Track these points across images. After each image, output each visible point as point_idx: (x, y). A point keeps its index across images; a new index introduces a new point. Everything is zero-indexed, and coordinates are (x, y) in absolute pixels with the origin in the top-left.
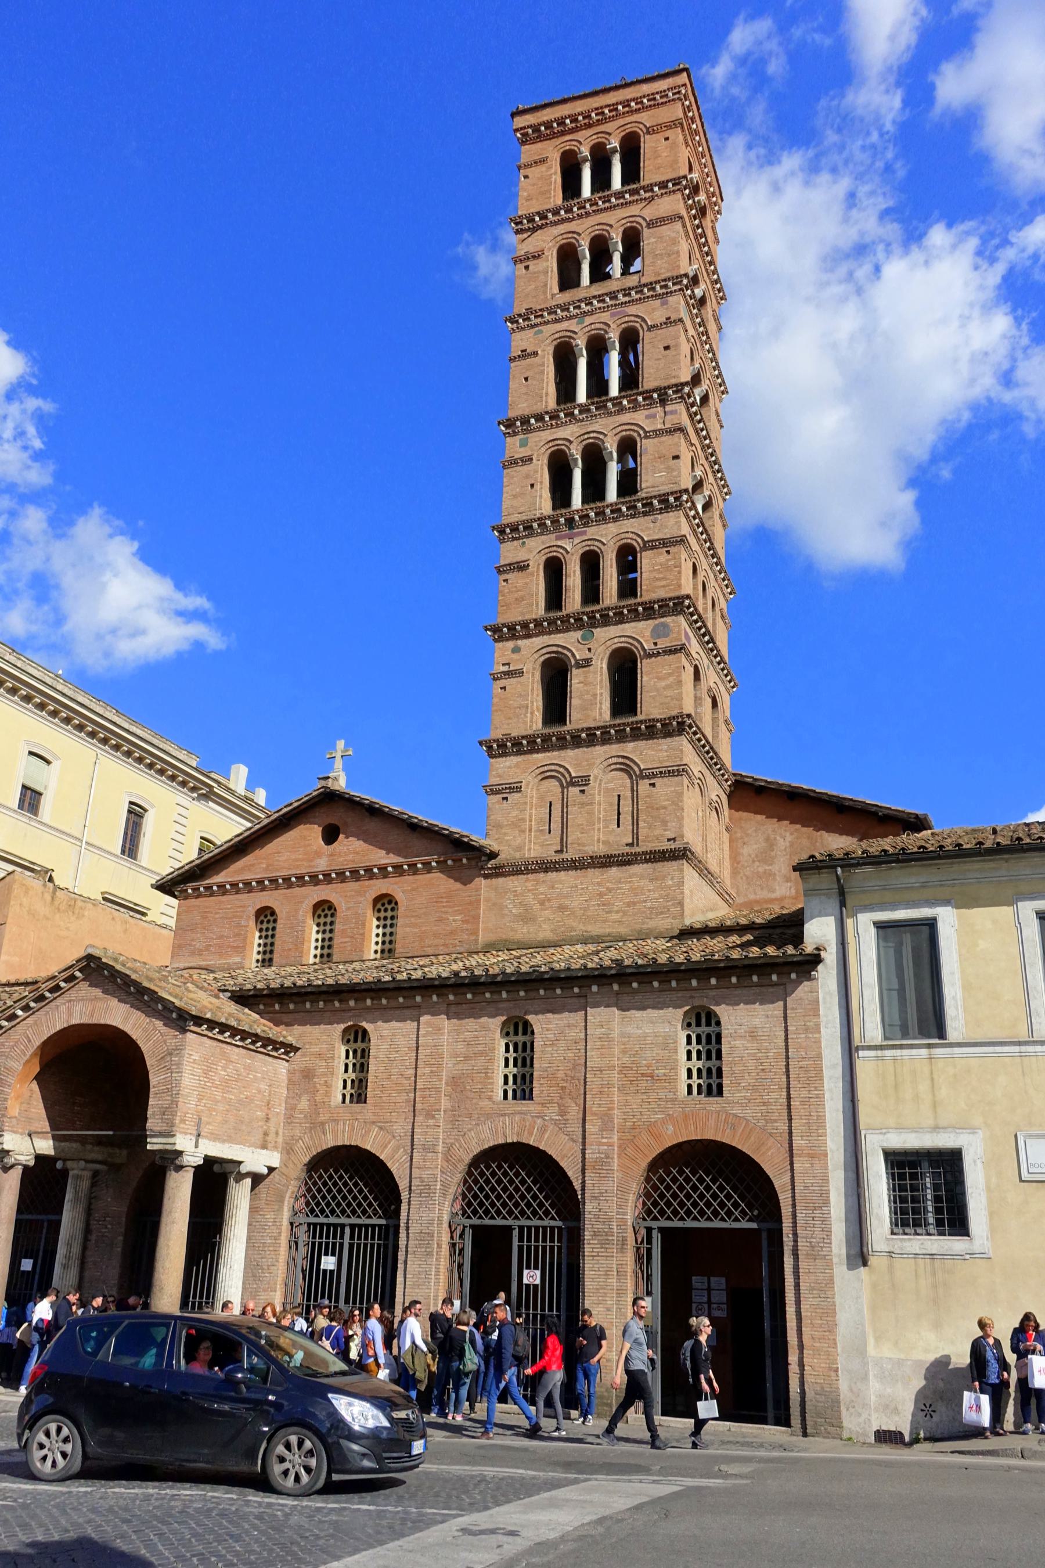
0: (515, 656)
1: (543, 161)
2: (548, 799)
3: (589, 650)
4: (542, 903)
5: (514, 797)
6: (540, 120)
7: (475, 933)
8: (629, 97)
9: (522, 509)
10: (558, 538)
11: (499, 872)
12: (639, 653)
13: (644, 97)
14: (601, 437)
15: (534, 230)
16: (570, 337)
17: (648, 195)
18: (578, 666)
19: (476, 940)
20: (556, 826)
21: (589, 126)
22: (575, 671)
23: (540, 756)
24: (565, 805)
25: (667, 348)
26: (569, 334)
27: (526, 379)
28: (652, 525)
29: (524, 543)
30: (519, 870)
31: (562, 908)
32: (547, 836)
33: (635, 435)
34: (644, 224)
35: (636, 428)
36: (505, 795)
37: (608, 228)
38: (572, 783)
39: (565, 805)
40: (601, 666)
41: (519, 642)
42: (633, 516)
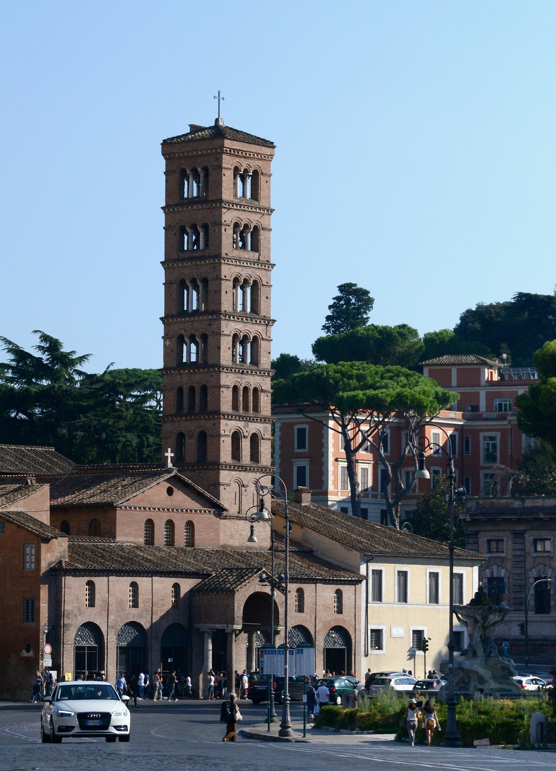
0: (226, 427)
1: (230, 169)
2: (235, 491)
3: (247, 432)
4: (236, 532)
5: (227, 488)
6: (232, 147)
7: (219, 541)
8: (259, 152)
9: (227, 359)
10: (237, 378)
11: (225, 518)
12: (260, 437)
13: (263, 154)
14: (249, 333)
15: (229, 209)
16: (239, 277)
17: (263, 212)
18: (245, 437)
19: (219, 544)
20: (237, 502)
21: (245, 157)
22: (243, 440)
23: (234, 473)
24: (240, 495)
25: (267, 298)
26: (239, 275)
27: (226, 292)
28: (263, 382)
29: (227, 376)
30: (231, 518)
31: (241, 535)
32: (235, 506)
33: (258, 336)
34: (261, 228)
35: (259, 334)
36: (225, 487)
37: (250, 222)
38: (243, 486)
39: (240, 495)
40: (249, 438)
41: (228, 422)
42: (259, 376)
